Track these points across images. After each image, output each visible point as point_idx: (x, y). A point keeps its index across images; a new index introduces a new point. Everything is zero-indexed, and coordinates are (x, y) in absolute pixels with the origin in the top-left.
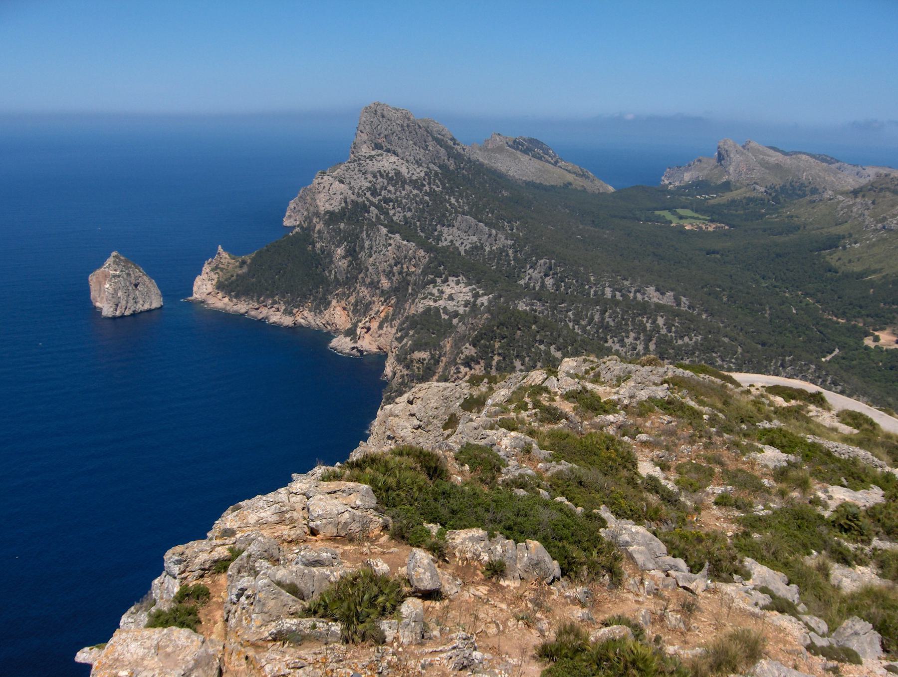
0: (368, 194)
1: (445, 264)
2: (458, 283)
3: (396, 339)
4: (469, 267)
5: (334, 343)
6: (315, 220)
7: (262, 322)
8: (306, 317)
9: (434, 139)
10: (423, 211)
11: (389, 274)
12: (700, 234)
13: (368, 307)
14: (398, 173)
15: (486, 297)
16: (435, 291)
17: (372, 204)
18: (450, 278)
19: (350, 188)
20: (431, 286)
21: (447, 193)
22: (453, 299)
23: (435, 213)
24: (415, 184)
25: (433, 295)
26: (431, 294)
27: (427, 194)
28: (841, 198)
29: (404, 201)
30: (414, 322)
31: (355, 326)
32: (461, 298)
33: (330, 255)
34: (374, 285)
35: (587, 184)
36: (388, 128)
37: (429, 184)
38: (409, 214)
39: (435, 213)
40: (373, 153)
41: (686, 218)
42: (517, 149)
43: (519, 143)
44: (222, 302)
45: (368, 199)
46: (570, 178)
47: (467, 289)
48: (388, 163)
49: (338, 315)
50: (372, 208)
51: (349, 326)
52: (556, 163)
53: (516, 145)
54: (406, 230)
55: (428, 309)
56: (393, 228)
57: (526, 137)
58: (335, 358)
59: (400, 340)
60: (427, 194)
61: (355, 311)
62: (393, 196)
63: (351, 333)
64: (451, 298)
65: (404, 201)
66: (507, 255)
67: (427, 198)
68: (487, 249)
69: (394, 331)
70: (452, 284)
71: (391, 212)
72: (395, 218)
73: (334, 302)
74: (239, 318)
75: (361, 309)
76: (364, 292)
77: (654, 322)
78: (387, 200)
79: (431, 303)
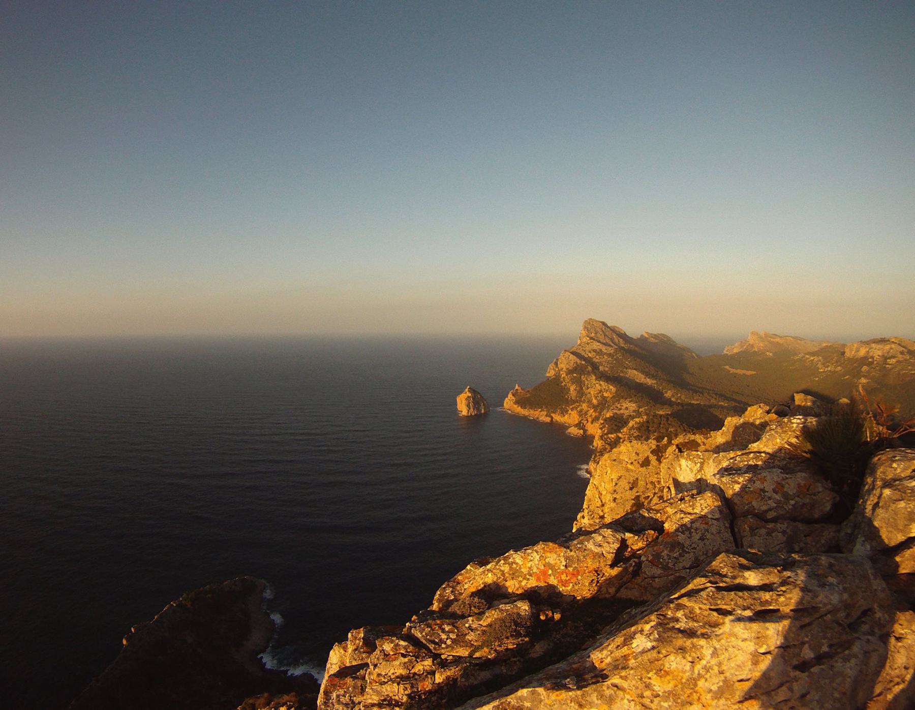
5: (569, 430)
8: (557, 418)
13: (586, 413)
24: (609, 355)
32: (632, 409)
34: (590, 402)
59: (601, 429)
64: (627, 408)
74: (525, 418)
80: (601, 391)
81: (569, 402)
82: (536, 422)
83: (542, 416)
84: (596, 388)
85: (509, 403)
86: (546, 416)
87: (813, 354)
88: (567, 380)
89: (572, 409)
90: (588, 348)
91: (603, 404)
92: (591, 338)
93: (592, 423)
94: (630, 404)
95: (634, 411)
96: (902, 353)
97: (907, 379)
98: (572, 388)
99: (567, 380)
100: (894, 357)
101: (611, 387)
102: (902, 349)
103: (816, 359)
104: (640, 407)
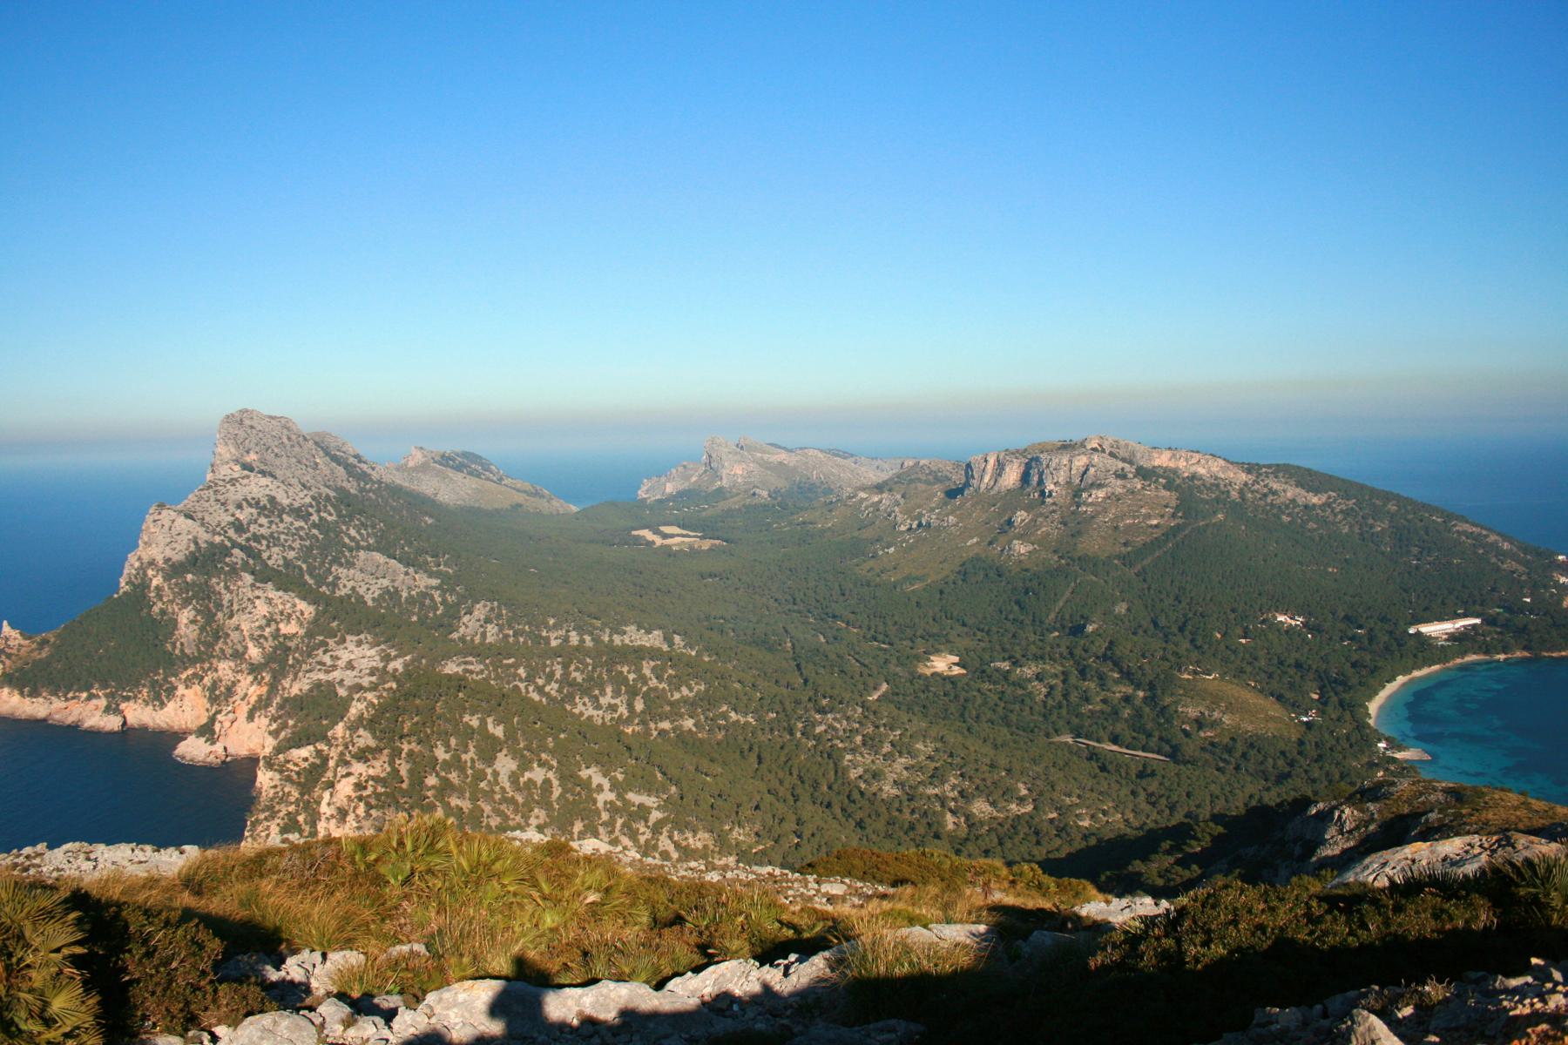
0: (231, 533)
1: (342, 617)
2: (359, 644)
3: (270, 733)
6: (150, 573)
8: (138, 713)
9: (327, 454)
10: (310, 549)
11: (258, 640)
12: (694, 553)
13: (230, 691)
14: (272, 499)
15: (400, 661)
16: (327, 659)
17: (235, 545)
18: (349, 638)
19: (203, 525)
20: (320, 651)
21: (344, 523)
22: (353, 668)
23: (329, 547)
24: (299, 513)
25: (324, 664)
26: (322, 663)
27: (315, 526)
28: (863, 495)
29: (283, 537)
30: (297, 705)
31: (212, 720)
32: (365, 664)
33: (174, 623)
34: (238, 655)
35: (543, 505)
36: (258, 439)
37: (318, 511)
38: (291, 555)
39: (329, 547)
40: (236, 475)
41: (672, 536)
42: (447, 465)
43: (449, 458)
45: (230, 539)
46: (519, 498)
47: (373, 652)
48: (258, 487)
49: (183, 709)
50: (236, 551)
51: (204, 720)
52: (501, 479)
53: (445, 460)
54: (286, 579)
55: (318, 685)
56: (264, 575)
57: (459, 449)
60: (315, 526)
61: (213, 699)
62: (263, 531)
63: (207, 731)
64: (350, 666)
65: (283, 537)
66: (432, 599)
67: (315, 531)
68: (404, 595)
69: (266, 721)
70: (351, 646)
71: (265, 555)
72: (270, 563)
73: (181, 690)
75: (220, 695)
76: (225, 669)
78: (256, 538)
79: (322, 676)
80: (270, 620)
82: (73, 732)
83: (90, 712)
84: (259, 611)
86: (107, 710)
87: (879, 488)
88: (168, 594)
89: (188, 683)
90: (235, 494)
91: (279, 660)
92: (247, 467)
93: (250, 717)
94: (358, 652)
95: (372, 672)
96: (1121, 476)
97: (1140, 540)
98: (185, 616)
99: (168, 594)
100: (1100, 486)
101: (302, 605)
102: (1120, 465)
103: (886, 499)
104: (387, 659)
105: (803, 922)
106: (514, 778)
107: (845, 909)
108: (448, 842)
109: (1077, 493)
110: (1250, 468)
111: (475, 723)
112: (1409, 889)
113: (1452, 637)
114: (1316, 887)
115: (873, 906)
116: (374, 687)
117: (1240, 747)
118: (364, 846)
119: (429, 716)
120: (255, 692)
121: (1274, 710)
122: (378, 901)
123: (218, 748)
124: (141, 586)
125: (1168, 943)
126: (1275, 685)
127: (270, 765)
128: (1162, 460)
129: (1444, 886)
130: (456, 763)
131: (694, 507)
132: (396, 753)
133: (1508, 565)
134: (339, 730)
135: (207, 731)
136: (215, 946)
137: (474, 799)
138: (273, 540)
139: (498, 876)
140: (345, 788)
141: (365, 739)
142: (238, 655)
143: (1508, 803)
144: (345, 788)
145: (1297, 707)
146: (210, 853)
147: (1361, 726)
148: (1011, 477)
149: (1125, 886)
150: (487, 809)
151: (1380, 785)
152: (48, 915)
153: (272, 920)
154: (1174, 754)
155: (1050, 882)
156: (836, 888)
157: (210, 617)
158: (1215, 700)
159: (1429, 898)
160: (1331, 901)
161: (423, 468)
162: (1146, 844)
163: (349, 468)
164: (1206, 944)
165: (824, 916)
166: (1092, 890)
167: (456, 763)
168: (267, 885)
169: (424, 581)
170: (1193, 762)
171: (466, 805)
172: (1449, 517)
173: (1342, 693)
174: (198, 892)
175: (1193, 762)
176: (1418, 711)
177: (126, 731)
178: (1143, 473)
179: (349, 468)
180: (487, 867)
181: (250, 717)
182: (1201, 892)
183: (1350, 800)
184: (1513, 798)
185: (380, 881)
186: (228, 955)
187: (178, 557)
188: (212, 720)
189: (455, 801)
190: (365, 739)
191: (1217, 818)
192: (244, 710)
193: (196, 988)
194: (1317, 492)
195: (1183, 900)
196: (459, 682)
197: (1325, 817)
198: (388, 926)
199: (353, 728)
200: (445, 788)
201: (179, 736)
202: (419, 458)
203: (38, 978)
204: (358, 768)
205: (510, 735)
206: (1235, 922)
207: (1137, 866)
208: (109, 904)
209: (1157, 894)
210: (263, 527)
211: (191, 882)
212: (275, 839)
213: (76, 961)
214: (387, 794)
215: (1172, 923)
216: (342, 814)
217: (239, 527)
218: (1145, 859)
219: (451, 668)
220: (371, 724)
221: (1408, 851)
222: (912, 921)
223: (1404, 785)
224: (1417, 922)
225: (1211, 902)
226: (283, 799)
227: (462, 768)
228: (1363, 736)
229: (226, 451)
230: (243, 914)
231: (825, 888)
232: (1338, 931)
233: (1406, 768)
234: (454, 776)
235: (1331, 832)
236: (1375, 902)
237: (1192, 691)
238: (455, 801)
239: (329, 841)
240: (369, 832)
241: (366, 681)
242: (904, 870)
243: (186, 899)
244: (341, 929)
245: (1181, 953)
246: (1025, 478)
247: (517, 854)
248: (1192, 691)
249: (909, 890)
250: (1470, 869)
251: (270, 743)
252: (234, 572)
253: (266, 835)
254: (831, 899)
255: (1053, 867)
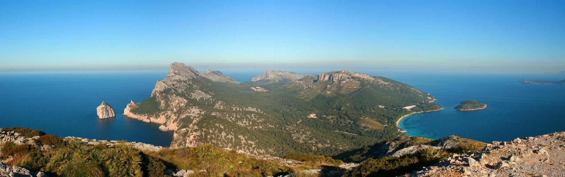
1: (192, 103)
4: (199, 104)
7: (141, 121)
8: (153, 120)
11: (176, 107)
13: (170, 117)
23: (190, 89)
24: (185, 82)
30: (183, 120)
31: (166, 122)
32: (196, 112)
34: (172, 110)
35: (233, 82)
39: (190, 89)
44: (132, 115)
46: (228, 80)
49: (161, 120)
53: (214, 72)
54: (182, 95)
55: (187, 116)
56: (178, 95)
58: (161, 132)
61: (167, 118)
63: (165, 124)
64: (194, 113)
74: (136, 120)
75: (168, 118)
76: (169, 113)
77: (251, 116)
81: (160, 111)
83: (145, 119)
84: (177, 102)
85: (127, 111)
87: (300, 80)
88: (160, 97)
90: (173, 79)
91: (180, 111)
93: (173, 123)
96: (349, 78)
97: (352, 91)
98: (162, 102)
99: (160, 97)
101: (185, 100)
104: (201, 112)
105: (283, 169)
106: (225, 137)
107: (292, 166)
108: (211, 149)
109: (340, 82)
110: (374, 77)
111: (218, 125)
112: (403, 157)
113: (411, 109)
114: (387, 158)
115: (298, 165)
116: (198, 117)
117: (373, 132)
118: (195, 149)
119: (209, 124)
120: (175, 118)
121: (379, 124)
122: (197, 160)
123: (167, 128)
124: (155, 95)
125: (359, 172)
126: (379, 119)
127: (176, 133)
128: (357, 75)
129: (409, 156)
130: (214, 133)
131: (264, 83)
132: (202, 131)
133: (420, 96)
134: (191, 125)
135: (165, 124)
136: (164, 167)
137: (217, 141)
138: (180, 87)
139: (222, 157)
140: (192, 137)
141: (196, 127)
142: (172, 110)
143: (421, 139)
144: (192, 137)
145: (383, 123)
146: (164, 148)
147: (395, 127)
148: (327, 78)
149: (349, 161)
150: (220, 143)
151: (399, 138)
152: (136, 155)
153: (175, 163)
154: (360, 134)
155: (334, 160)
156: (290, 162)
157: (167, 102)
158: (368, 123)
159: (407, 158)
160: (389, 161)
161: (209, 74)
162: (354, 152)
163: (195, 73)
164: (366, 172)
165: (287, 167)
166: (342, 162)
167: (214, 133)
168: (175, 156)
169: (209, 96)
170: (364, 135)
171: (215, 142)
172: (410, 87)
173: (391, 120)
174: (162, 156)
175: (364, 135)
176: (405, 123)
177: (150, 123)
178: (353, 78)
179: (195, 73)
180: (219, 155)
181: (173, 123)
182: (365, 161)
183: (393, 141)
184: (422, 138)
185: (198, 156)
186: (167, 168)
187: (162, 90)
188: (166, 122)
189: (213, 141)
190: (196, 127)
191: (369, 146)
192: (172, 121)
193: (160, 174)
194: (387, 82)
195: (361, 163)
196: (215, 117)
197: (389, 145)
198: (199, 166)
199: (194, 125)
200: (211, 138)
201: (160, 125)
202: (209, 72)
203: (134, 166)
204: (194, 133)
205: (225, 128)
206: (371, 167)
207: (351, 157)
208: (146, 155)
209: (355, 162)
210: (178, 85)
211: (160, 153)
212: (177, 148)
213: (140, 164)
214: (200, 139)
215: (359, 168)
216: (191, 142)
217: (173, 85)
218: (353, 155)
219: (213, 114)
220: (197, 125)
221: (404, 150)
222: (305, 169)
223: (403, 137)
224: (405, 163)
225: (367, 163)
226: (178, 139)
227: (215, 135)
228: (395, 128)
229: (172, 70)
230: (170, 161)
231: (288, 162)
232: (391, 167)
233: (403, 134)
234: (213, 136)
235: (390, 147)
236: (397, 160)
237: (363, 121)
238: (213, 141)
239: (188, 148)
240: (196, 146)
241: (196, 116)
242: (304, 158)
243: (159, 157)
244: (190, 166)
245: (361, 174)
246: (330, 78)
247: (225, 152)
248: (363, 121)
249: (305, 162)
250: (414, 152)
251: (177, 128)
252: (172, 94)
253: (175, 146)
254: (289, 164)
255: (334, 157)
